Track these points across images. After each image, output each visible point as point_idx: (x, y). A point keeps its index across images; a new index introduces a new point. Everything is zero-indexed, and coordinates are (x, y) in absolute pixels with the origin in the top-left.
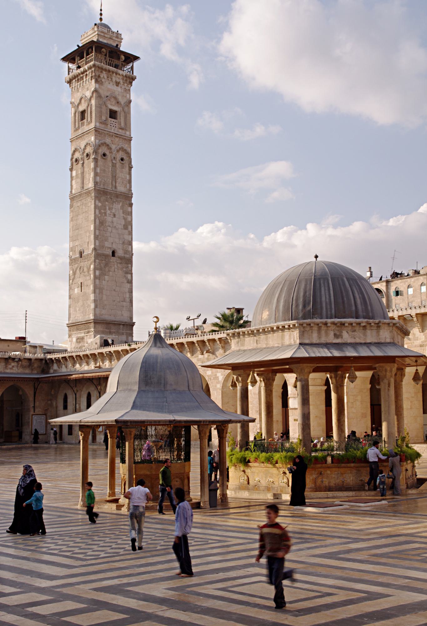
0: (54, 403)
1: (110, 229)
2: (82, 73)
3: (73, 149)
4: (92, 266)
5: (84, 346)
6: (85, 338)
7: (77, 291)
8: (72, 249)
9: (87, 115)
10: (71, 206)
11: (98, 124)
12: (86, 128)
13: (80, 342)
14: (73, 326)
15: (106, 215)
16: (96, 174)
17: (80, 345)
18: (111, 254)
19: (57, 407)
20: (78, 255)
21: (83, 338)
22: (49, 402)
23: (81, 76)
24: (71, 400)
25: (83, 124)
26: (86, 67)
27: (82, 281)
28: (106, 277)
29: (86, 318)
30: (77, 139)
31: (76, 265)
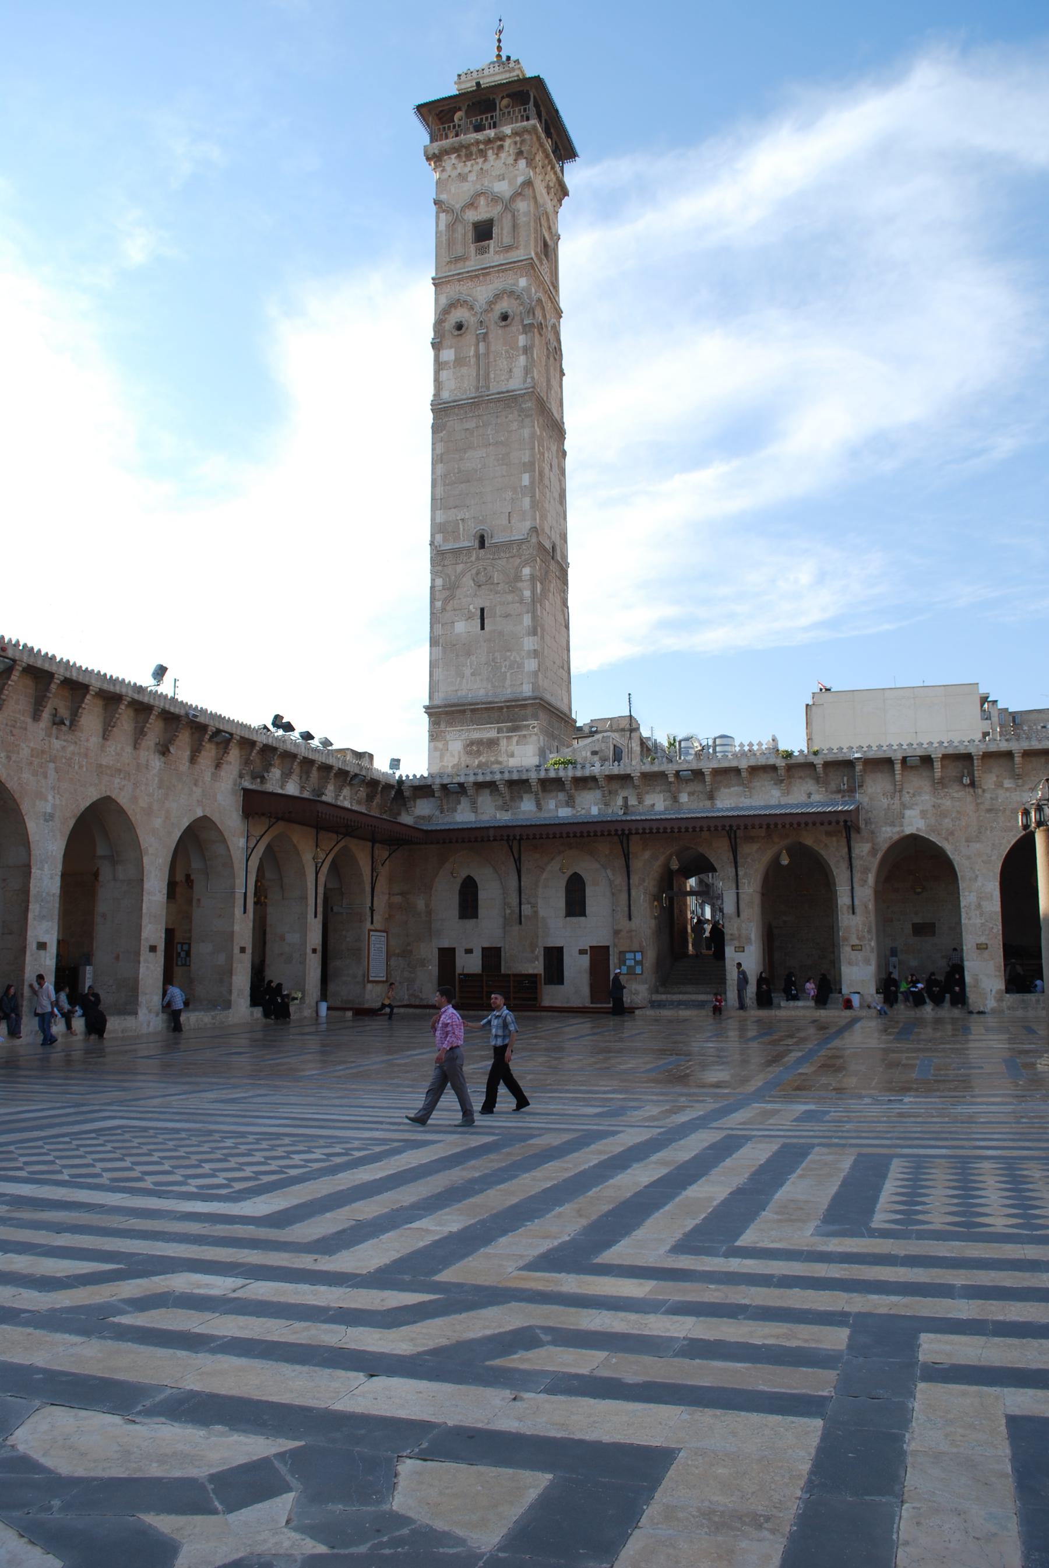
0: (421, 904)
2: (489, 141)
3: (443, 300)
4: (526, 571)
5: (500, 763)
6: (503, 743)
7: (463, 628)
8: (437, 528)
9: (502, 232)
10: (436, 429)
11: (533, 255)
13: (479, 753)
14: (444, 715)
17: (483, 759)
19: (429, 913)
20: (468, 542)
21: (492, 743)
22: (398, 899)
23: (482, 147)
24: (489, 893)
25: (483, 251)
26: (507, 130)
27: (486, 604)
29: (507, 692)
30: (459, 280)
31: (460, 568)
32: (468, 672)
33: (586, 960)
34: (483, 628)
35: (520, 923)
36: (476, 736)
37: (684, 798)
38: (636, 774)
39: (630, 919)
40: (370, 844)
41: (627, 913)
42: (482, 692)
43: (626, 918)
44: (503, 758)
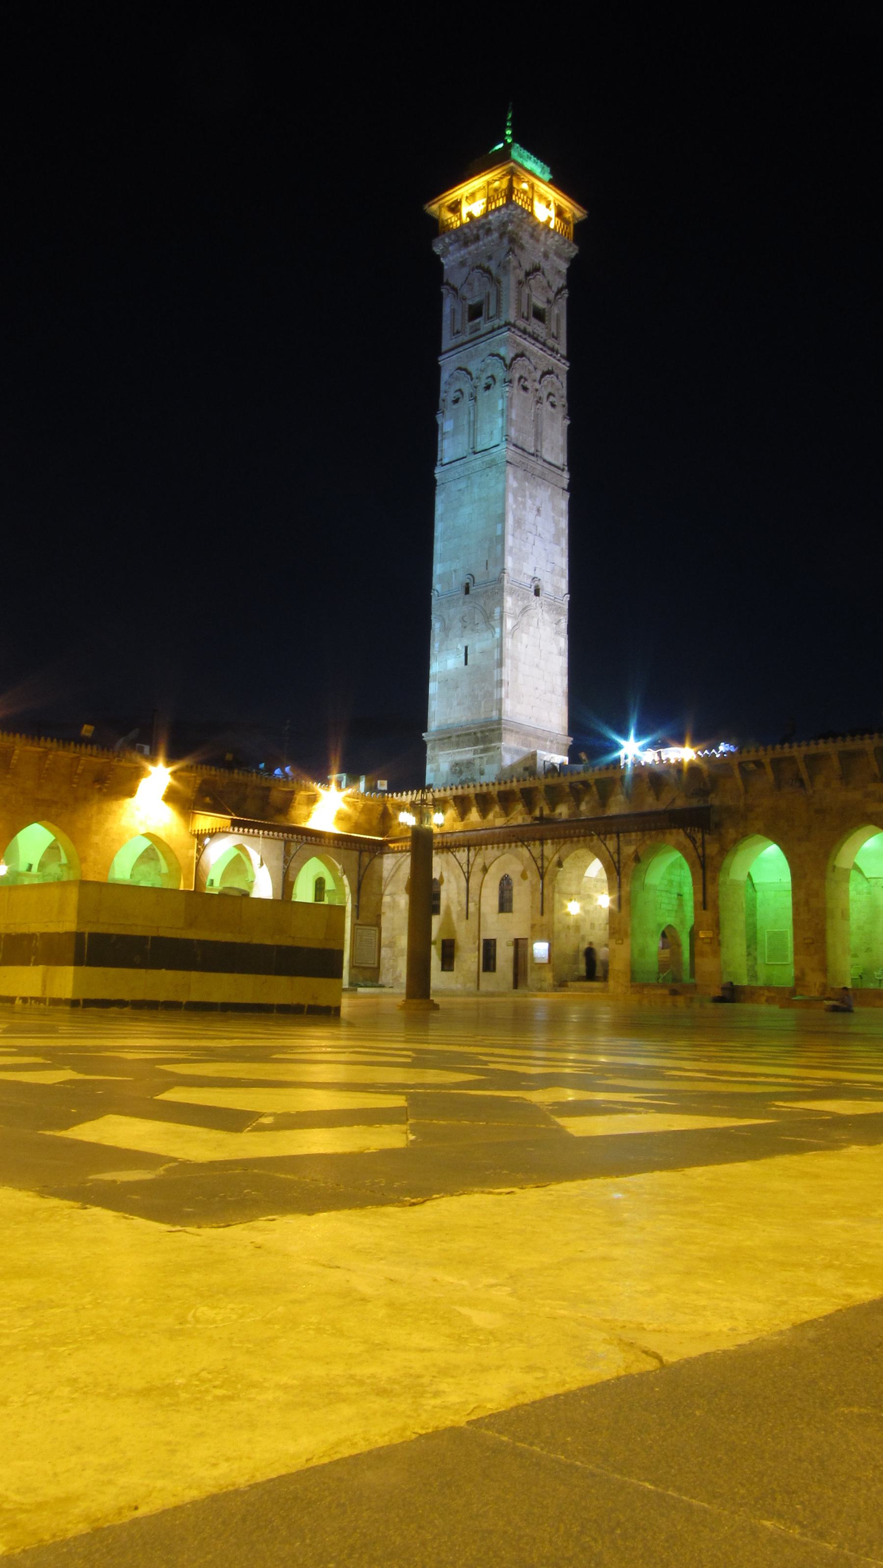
1: (531, 537)
12: (485, 326)
15: (524, 508)
16: (509, 422)
18: (533, 589)
28: (524, 636)
32: (455, 703)
33: (510, 951)
34: (466, 664)
35: (467, 918)
36: (458, 758)
37: (583, 807)
38: (517, 790)
39: (542, 914)
40: (356, 854)
41: (540, 910)
42: (464, 719)
43: (539, 914)
44: (477, 776)
